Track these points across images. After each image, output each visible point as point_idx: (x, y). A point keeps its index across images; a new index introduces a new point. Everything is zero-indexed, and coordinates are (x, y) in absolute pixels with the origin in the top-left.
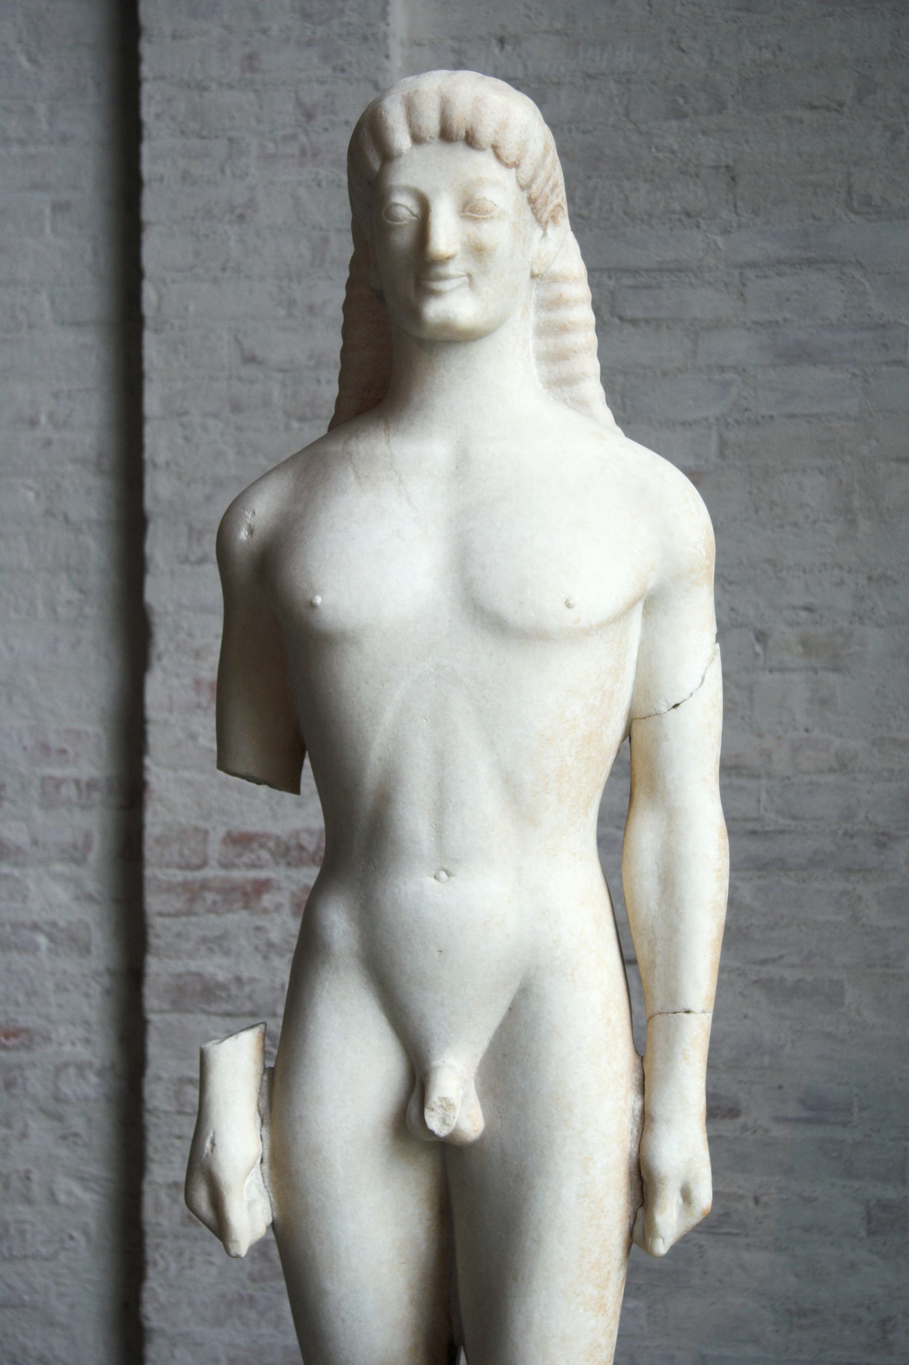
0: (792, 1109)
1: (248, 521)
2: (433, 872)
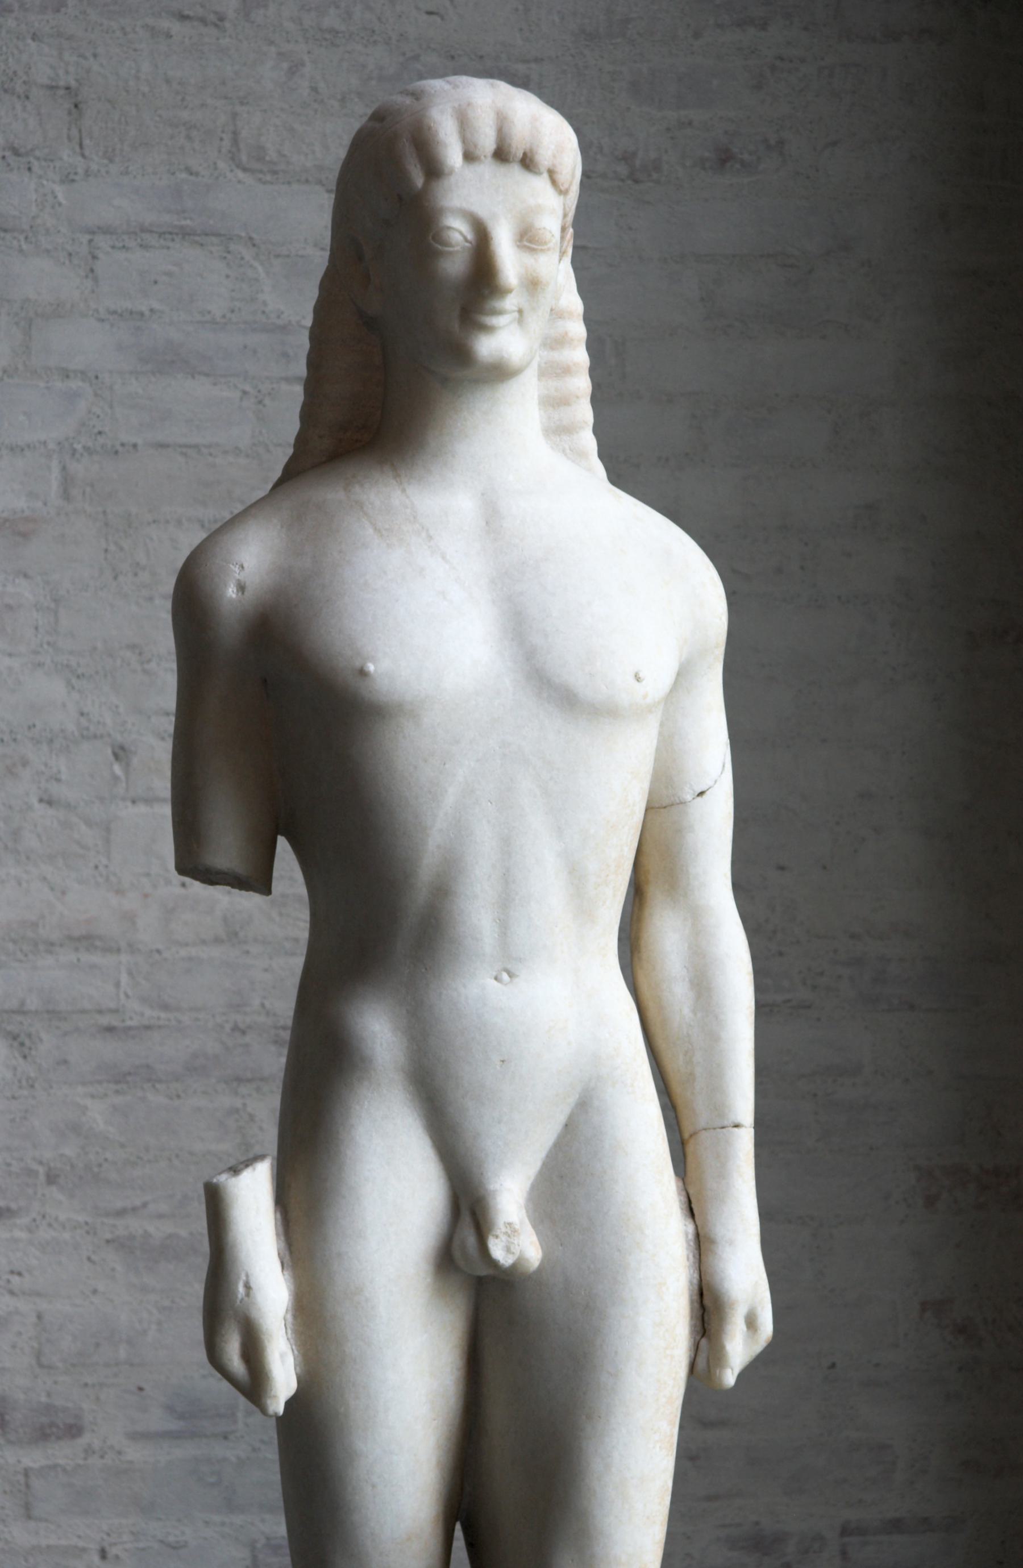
0: (157, 1420)
1: (237, 575)
2: (494, 974)
